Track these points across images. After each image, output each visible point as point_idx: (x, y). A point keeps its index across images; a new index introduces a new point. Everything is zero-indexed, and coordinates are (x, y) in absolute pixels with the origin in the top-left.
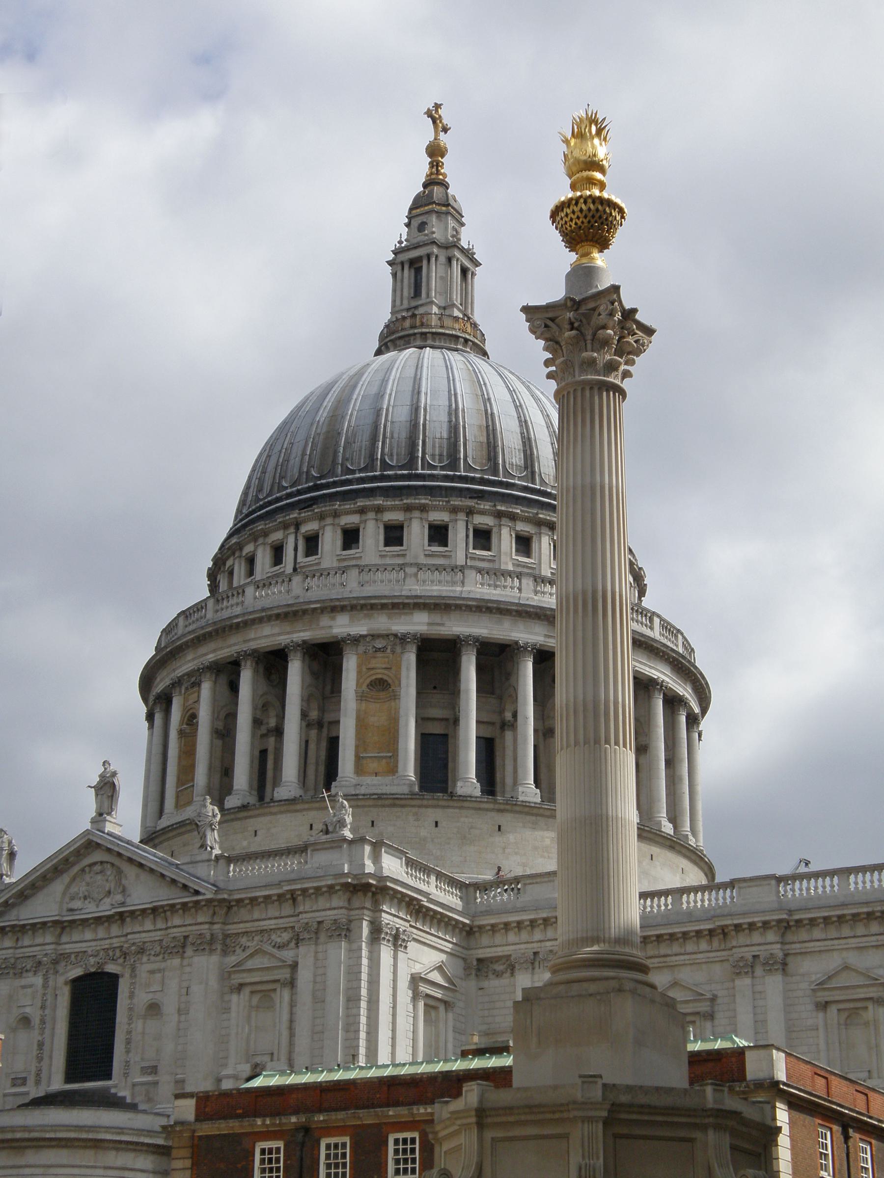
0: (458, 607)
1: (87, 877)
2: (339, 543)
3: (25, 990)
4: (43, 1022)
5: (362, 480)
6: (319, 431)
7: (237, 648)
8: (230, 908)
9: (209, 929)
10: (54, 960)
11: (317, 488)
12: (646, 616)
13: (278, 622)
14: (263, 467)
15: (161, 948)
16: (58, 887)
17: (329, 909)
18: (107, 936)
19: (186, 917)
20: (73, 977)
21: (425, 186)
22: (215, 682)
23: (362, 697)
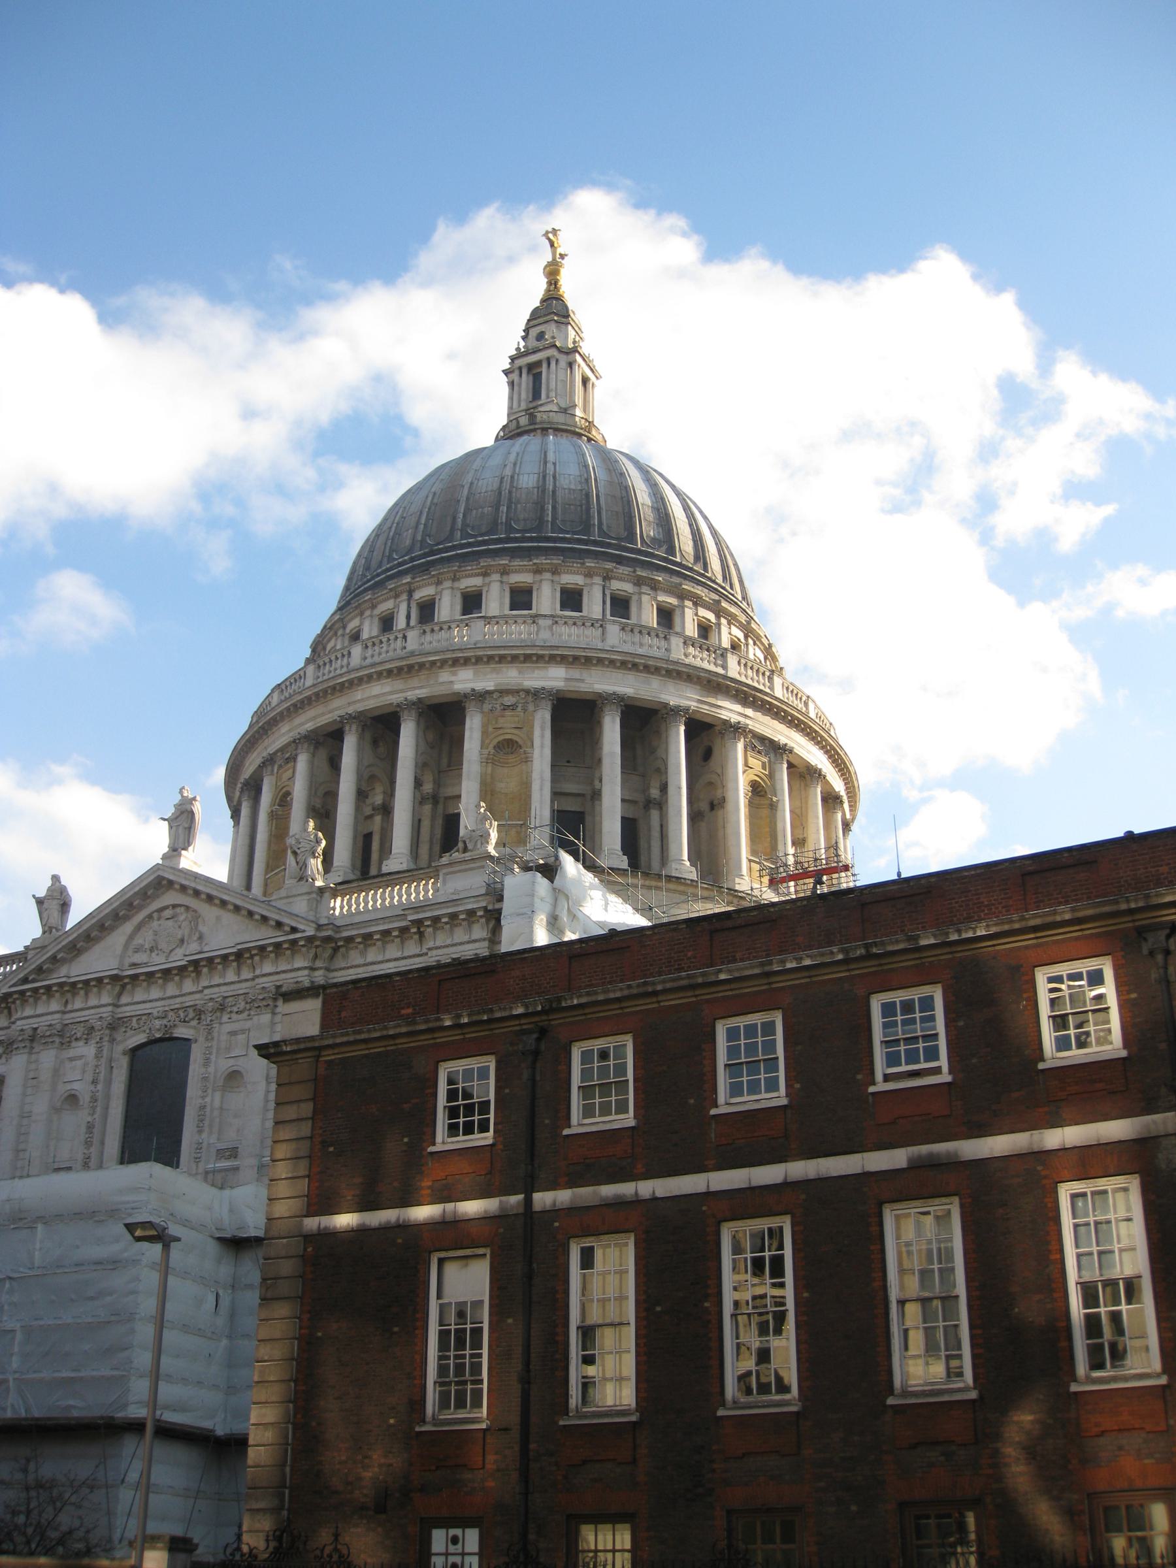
0: (600, 661)
1: (155, 924)
2: (458, 607)
3: (74, 1062)
4: (94, 1099)
5: (484, 543)
6: (435, 501)
7: (342, 712)
8: (336, 950)
9: (309, 976)
10: (110, 1024)
11: (432, 553)
12: (801, 699)
13: (389, 680)
14: (371, 546)
15: (247, 1003)
16: (118, 938)
17: (468, 942)
18: (178, 993)
19: (279, 963)
20: (133, 1045)
21: (543, 301)
22: (314, 755)
23: (487, 759)
